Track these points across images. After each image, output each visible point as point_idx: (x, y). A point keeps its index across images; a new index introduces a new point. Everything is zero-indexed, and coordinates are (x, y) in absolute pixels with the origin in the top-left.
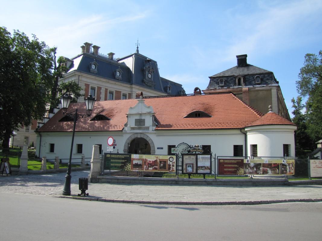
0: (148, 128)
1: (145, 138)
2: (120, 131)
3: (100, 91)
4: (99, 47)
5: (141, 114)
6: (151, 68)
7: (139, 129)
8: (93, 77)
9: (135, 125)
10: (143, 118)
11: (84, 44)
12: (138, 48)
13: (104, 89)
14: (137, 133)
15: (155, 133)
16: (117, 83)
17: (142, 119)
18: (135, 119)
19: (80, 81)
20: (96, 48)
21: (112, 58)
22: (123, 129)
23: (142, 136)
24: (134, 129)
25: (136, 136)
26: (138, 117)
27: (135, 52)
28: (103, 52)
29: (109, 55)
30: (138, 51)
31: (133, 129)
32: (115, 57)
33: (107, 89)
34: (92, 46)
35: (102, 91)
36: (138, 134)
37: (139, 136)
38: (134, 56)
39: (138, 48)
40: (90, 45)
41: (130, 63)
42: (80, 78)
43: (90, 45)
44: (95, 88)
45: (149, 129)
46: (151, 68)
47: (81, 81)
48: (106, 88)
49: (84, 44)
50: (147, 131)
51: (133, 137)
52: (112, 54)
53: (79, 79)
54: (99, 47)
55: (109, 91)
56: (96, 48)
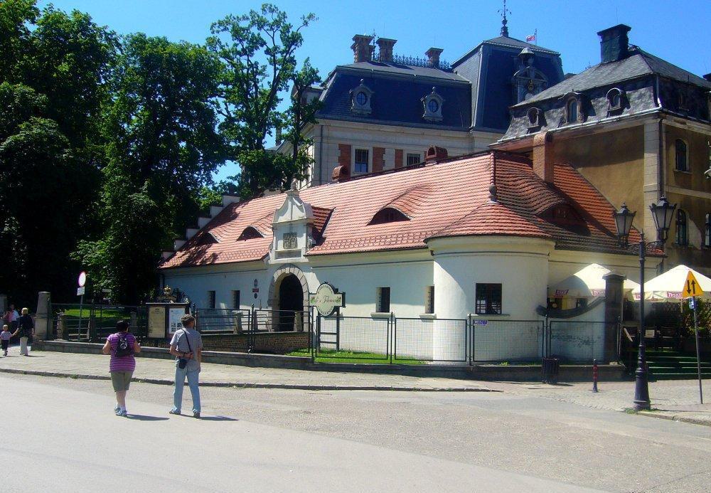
2: (258, 260)
3: (382, 157)
4: (394, 42)
6: (533, 74)
8: (361, 125)
11: (353, 39)
12: (505, 22)
13: (393, 152)
16: (427, 131)
19: (324, 140)
20: (387, 45)
21: (435, 64)
22: (264, 257)
27: (494, 34)
28: (410, 49)
29: (429, 56)
30: (505, 31)
31: (280, 255)
32: (447, 58)
33: (402, 151)
34: (376, 39)
35: (385, 157)
38: (481, 49)
39: (505, 22)
40: (369, 39)
41: (471, 73)
42: (325, 132)
43: (367, 39)
44: (368, 151)
46: (533, 74)
47: (328, 137)
48: (399, 148)
49: (353, 39)
52: (434, 53)
53: (321, 134)
54: (394, 42)
55: (408, 154)
56: (387, 45)
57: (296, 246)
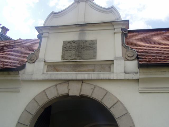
0: (108, 65)
1: (97, 96)
5: (83, 26)
7: (77, 67)
9: (63, 57)
10: (90, 36)
14: (68, 81)
15: (137, 80)
17: (86, 41)
18: (64, 41)
23: (87, 91)
24: (57, 71)
25: (63, 90)
26: (73, 36)
31: (53, 66)
36: (71, 83)
37: (74, 91)
45: (110, 68)
50: (105, 75)
51: (52, 94)
57: (95, 56)
